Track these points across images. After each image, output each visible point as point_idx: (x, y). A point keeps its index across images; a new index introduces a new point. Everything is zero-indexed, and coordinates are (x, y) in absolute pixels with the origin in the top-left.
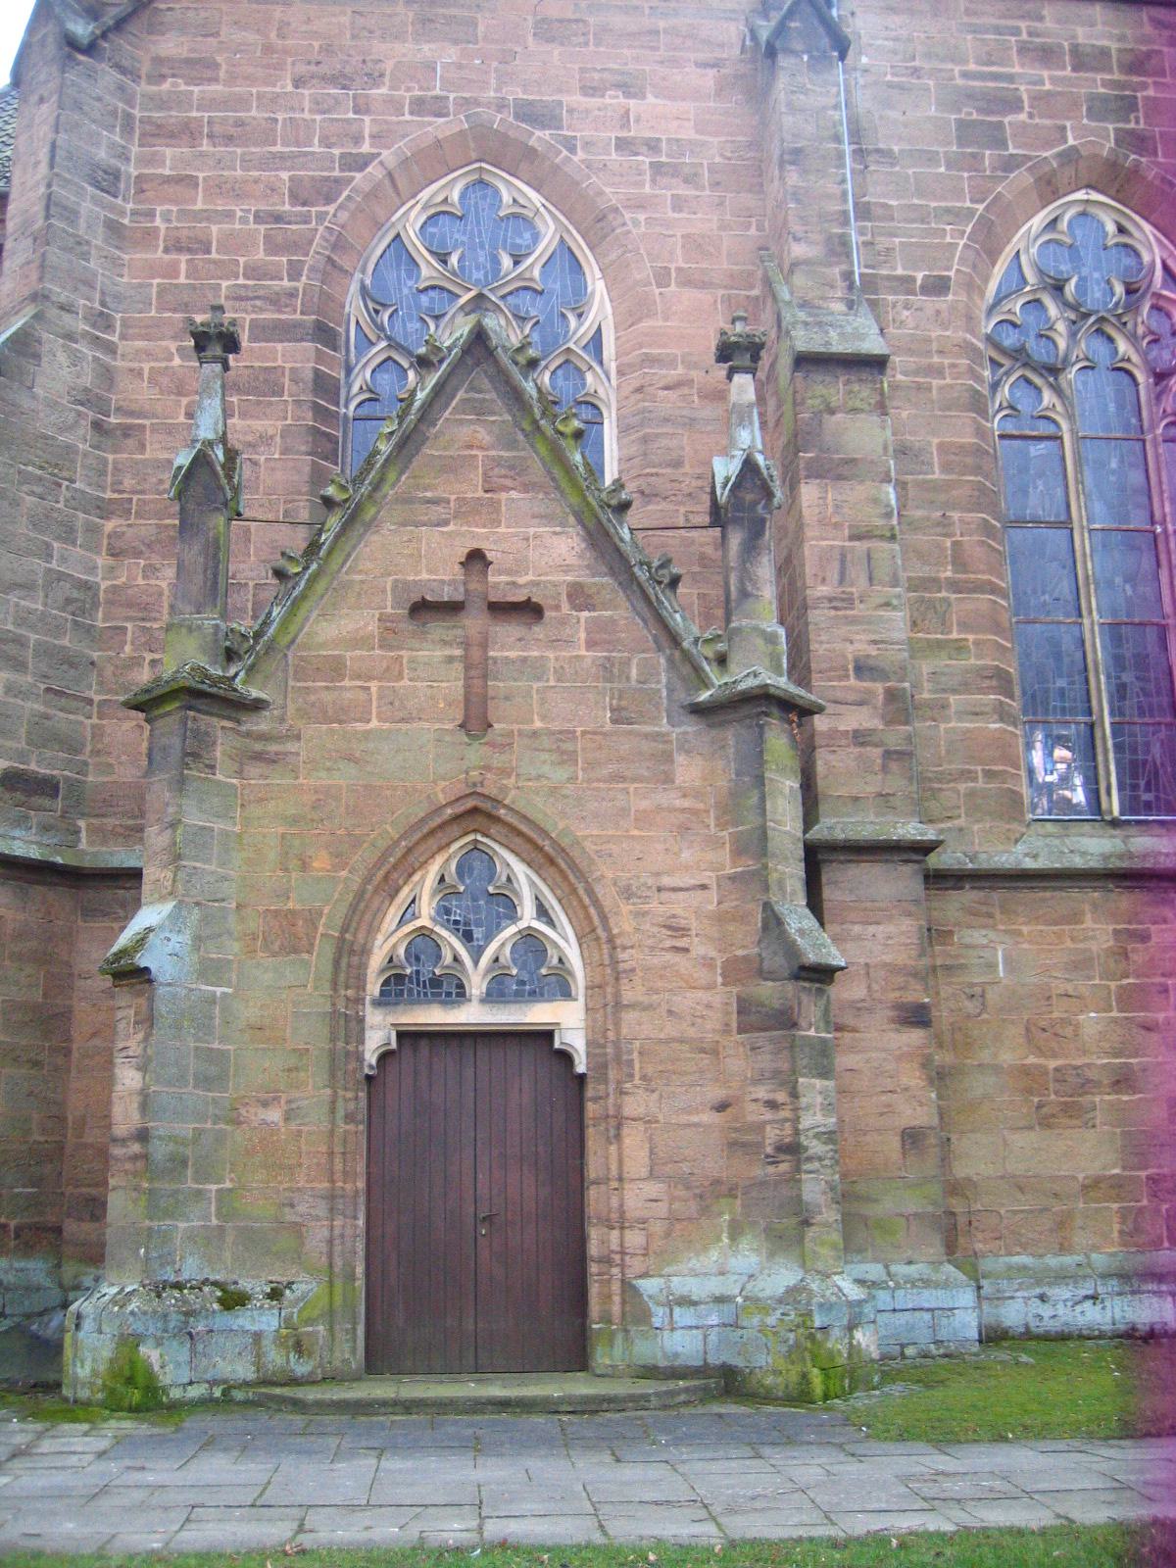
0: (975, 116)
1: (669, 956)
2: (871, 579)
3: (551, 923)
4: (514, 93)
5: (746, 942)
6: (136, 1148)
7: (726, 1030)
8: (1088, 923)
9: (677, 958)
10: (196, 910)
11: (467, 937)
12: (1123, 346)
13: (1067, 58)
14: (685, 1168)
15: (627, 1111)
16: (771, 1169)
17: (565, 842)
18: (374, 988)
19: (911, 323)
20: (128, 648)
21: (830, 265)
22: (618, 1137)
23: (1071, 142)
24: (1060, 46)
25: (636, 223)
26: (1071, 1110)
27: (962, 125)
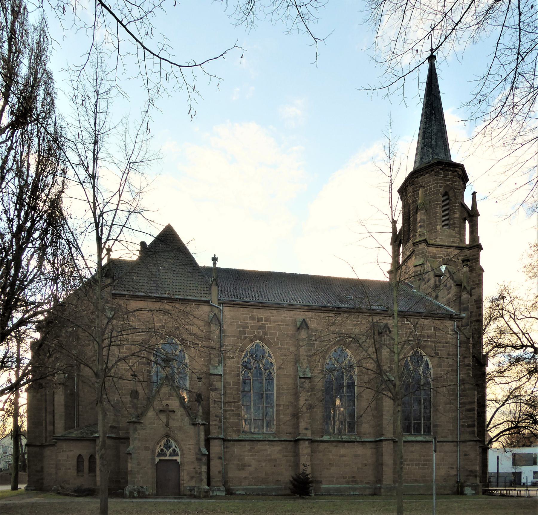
18: (156, 455)
27: (240, 331)
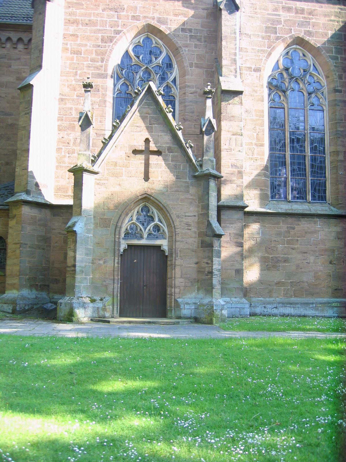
0: (270, 26)
1: (186, 231)
2: (236, 145)
3: (161, 222)
4: (156, 15)
5: (204, 229)
6: (73, 268)
7: (198, 247)
8: (281, 225)
9: (189, 231)
10: (85, 218)
11: (143, 225)
12: (301, 85)
13: (294, 11)
14: (188, 276)
15: (177, 263)
16: (207, 277)
17: (165, 205)
18: (123, 235)
20: (63, 153)
21: (231, 66)
22: (175, 269)
23: (293, 33)
24: (292, 7)
25: (185, 51)
26: (274, 267)
27: (266, 27)
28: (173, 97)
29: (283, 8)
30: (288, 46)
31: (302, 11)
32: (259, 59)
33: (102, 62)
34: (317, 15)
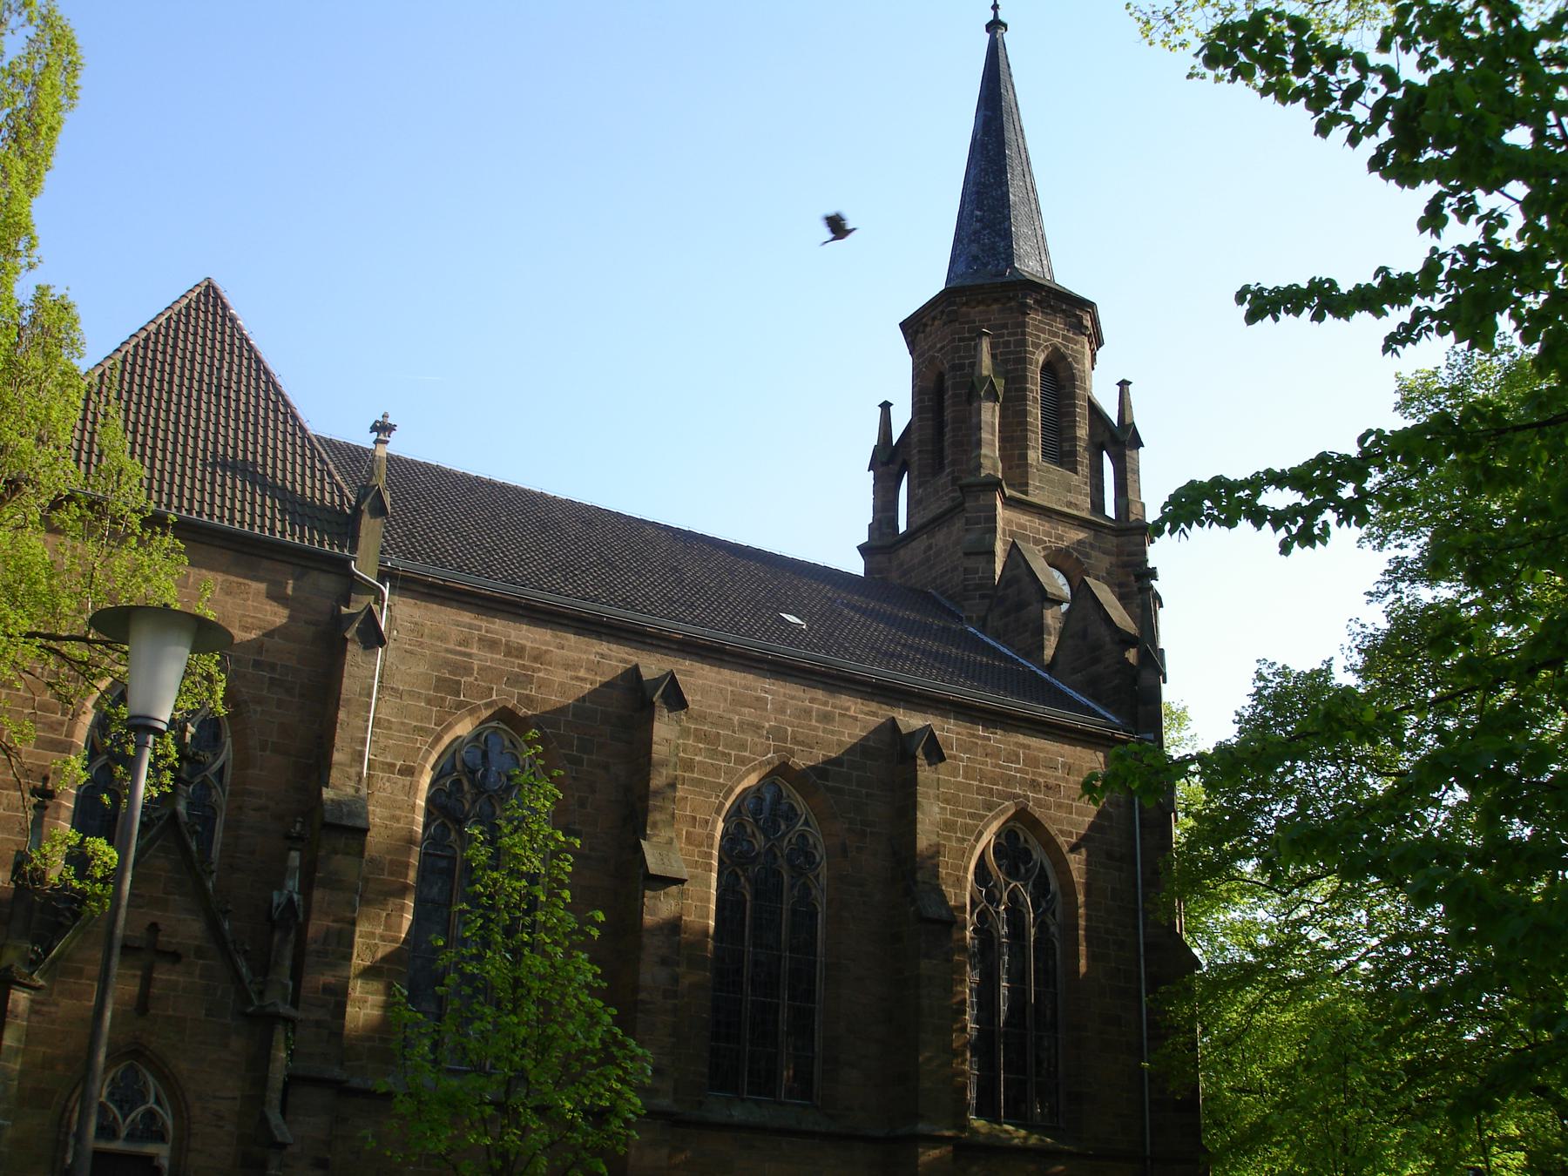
11: (120, 1108)
13: (502, 648)
19: (389, 790)
21: (351, 766)
23: (494, 697)
24: (501, 640)
27: (439, 679)
28: (213, 809)
29: (479, 639)
30: (481, 723)
31: (519, 651)
32: (414, 747)
33: (64, 714)
34: (550, 664)
